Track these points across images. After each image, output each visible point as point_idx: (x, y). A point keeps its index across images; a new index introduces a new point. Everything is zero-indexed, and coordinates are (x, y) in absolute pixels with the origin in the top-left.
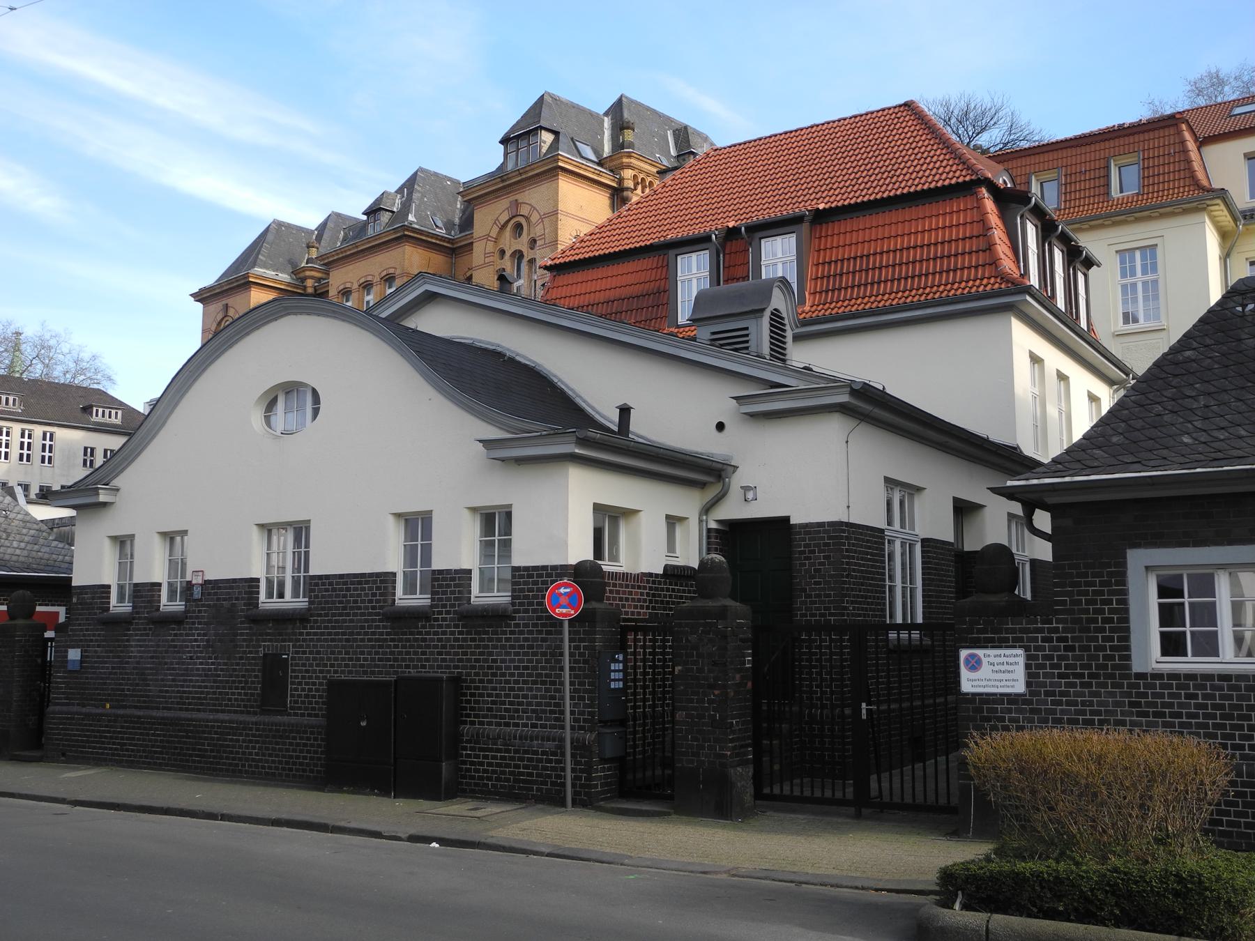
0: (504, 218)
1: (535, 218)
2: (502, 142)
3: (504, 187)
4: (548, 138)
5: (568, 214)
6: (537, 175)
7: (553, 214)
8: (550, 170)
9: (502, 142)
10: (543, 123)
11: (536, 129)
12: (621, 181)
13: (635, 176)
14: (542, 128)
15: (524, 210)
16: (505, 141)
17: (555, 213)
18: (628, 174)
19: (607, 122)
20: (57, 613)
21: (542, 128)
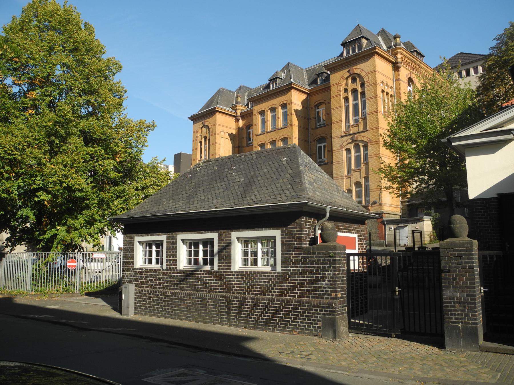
0: (347, 74)
1: (363, 74)
2: (342, 45)
3: (347, 62)
4: (364, 41)
5: (379, 72)
6: (368, 54)
7: (374, 71)
8: (370, 54)
9: (342, 45)
10: (365, 36)
11: (360, 38)
12: (397, 59)
13: (402, 58)
14: (363, 37)
15: (358, 72)
16: (343, 45)
17: (374, 71)
18: (399, 56)
19: (380, 38)
20: (355, 238)
21: (363, 37)
